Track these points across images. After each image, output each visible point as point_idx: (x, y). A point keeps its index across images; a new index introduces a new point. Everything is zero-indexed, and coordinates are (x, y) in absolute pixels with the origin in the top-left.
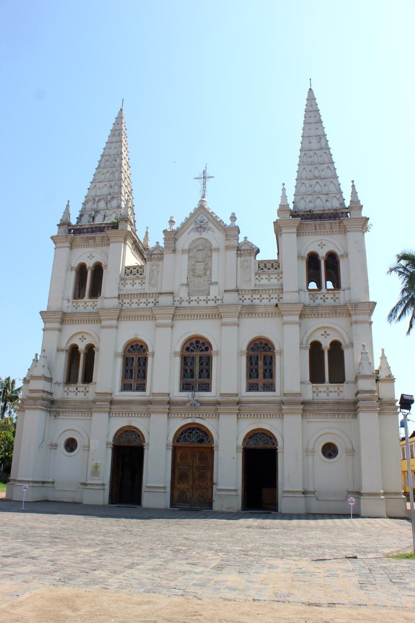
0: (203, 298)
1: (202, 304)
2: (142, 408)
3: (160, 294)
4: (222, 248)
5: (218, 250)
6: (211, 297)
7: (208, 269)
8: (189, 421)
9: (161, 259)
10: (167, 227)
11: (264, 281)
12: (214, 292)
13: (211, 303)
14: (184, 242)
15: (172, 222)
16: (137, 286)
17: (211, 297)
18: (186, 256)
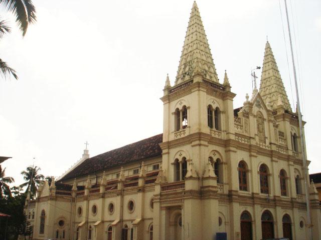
0: (264, 144)
1: (264, 147)
2: (250, 201)
3: (250, 137)
4: (267, 120)
5: (266, 119)
6: (267, 145)
7: (263, 129)
8: (265, 209)
9: (248, 117)
10: (245, 100)
11: (281, 142)
12: (267, 141)
13: (267, 148)
14: (255, 110)
15: (247, 97)
16: (239, 130)
17: (267, 145)
18: (255, 119)
